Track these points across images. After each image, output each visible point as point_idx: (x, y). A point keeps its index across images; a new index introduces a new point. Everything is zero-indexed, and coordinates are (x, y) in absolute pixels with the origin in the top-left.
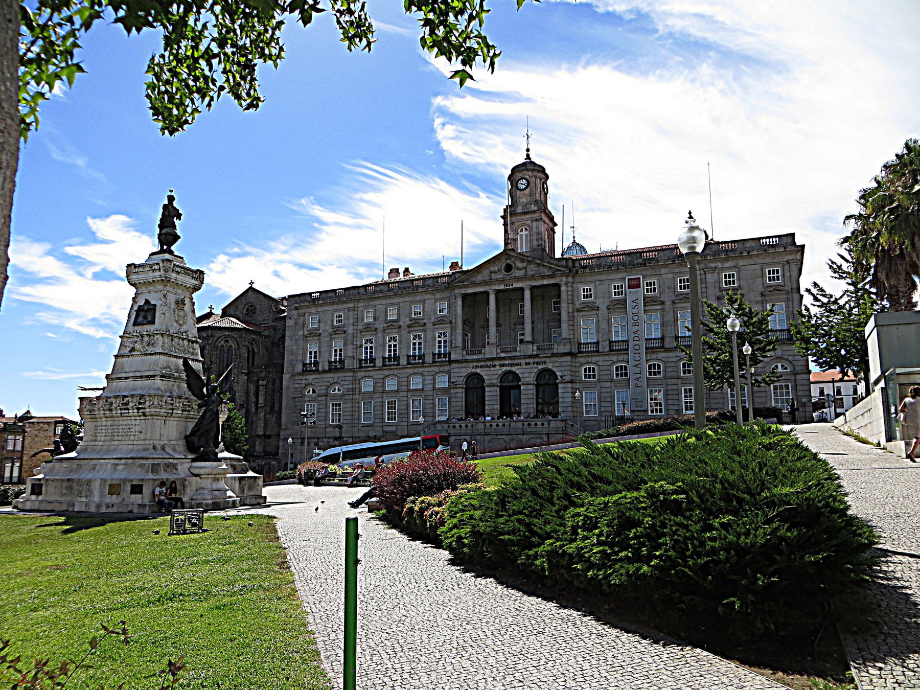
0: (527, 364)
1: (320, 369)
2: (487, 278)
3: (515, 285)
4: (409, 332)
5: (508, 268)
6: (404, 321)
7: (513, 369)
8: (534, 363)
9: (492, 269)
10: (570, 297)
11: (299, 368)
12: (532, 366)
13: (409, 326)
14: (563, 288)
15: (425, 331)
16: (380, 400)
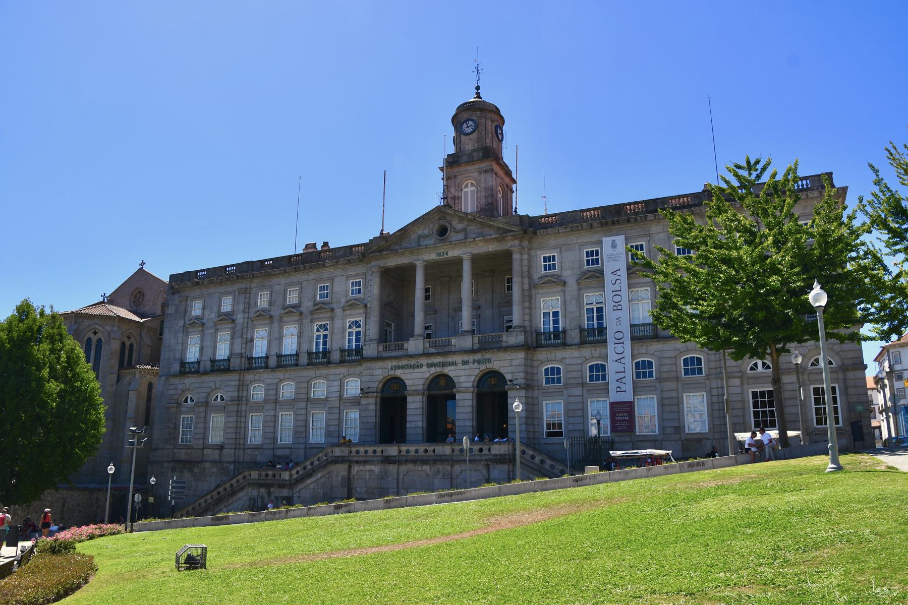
0: (465, 363)
1: (201, 370)
3: (454, 253)
4: (312, 321)
5: (443, 232)
6: (307, 305)
7: (447, 370)
8: (474, 361)
9: (420, 232)
10: (525, 269)
11: (176, 367)
12: (471, 364)
13: (312, 313)
14: (516, 256)
15: (332, 319)
16: (272, 413)
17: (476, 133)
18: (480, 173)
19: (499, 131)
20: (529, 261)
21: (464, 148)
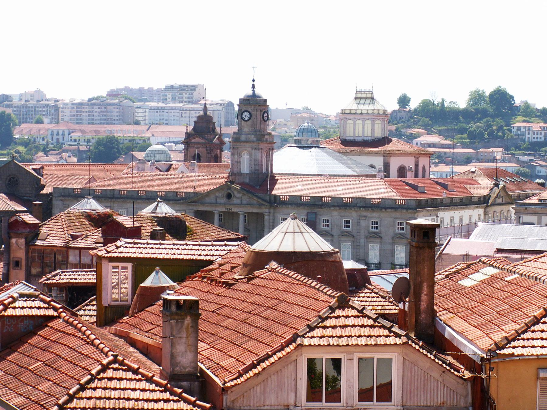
2: (214, 201)
3: (234, 210)
9: (217, 194)
14: (266, 217)
17: (251, 120)
18: (252, 149)
19: (266, 115)
20: (274, 219)
21: (243, 129)
